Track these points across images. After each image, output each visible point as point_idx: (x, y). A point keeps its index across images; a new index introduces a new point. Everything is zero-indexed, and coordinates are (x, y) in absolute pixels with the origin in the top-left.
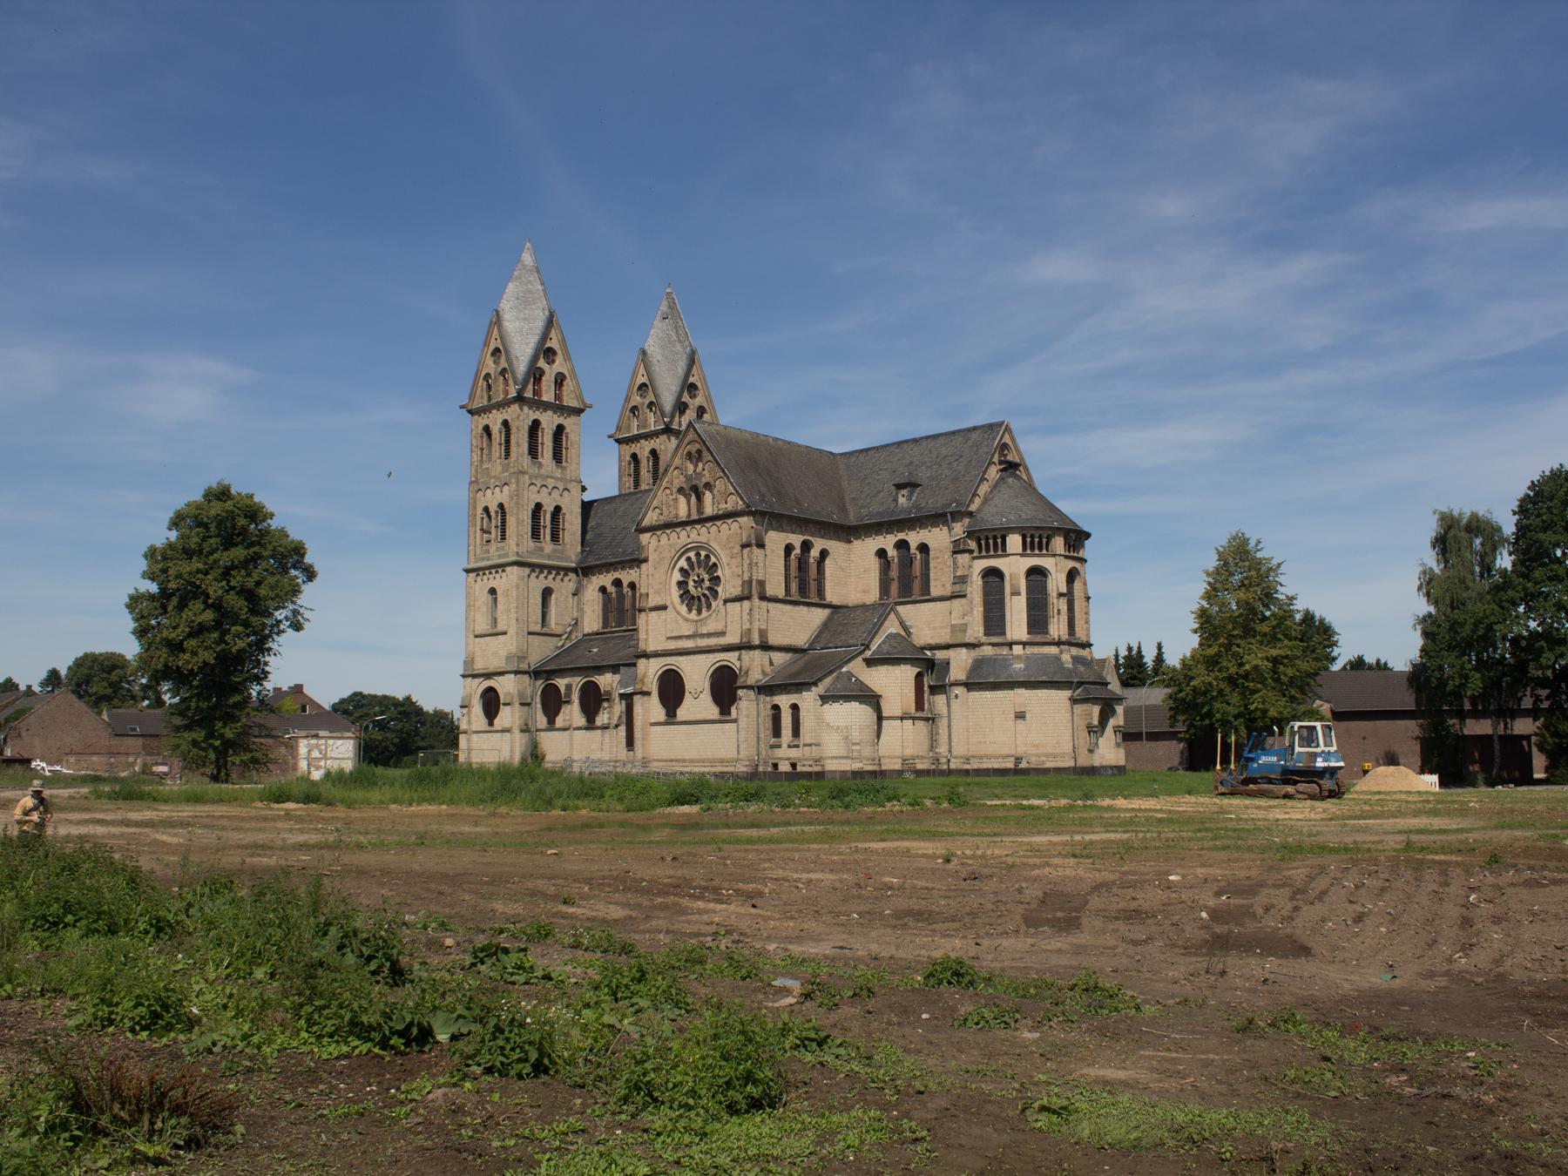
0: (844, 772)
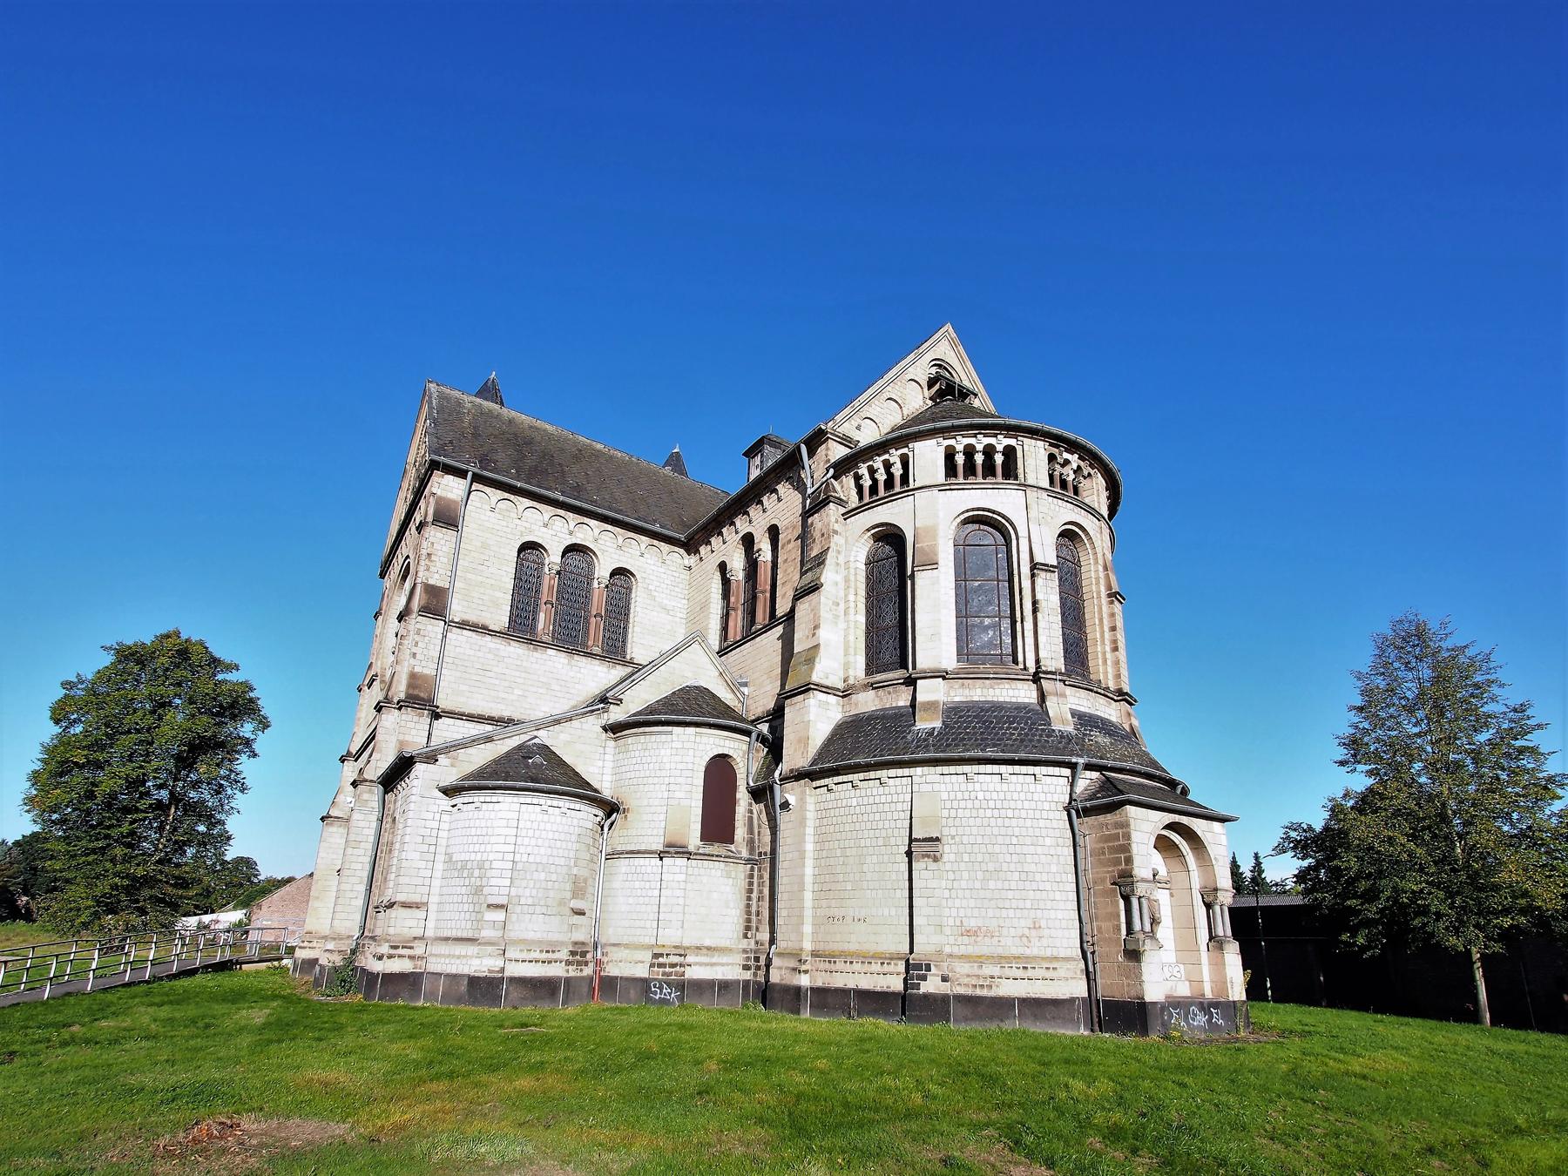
0: (454, 978)
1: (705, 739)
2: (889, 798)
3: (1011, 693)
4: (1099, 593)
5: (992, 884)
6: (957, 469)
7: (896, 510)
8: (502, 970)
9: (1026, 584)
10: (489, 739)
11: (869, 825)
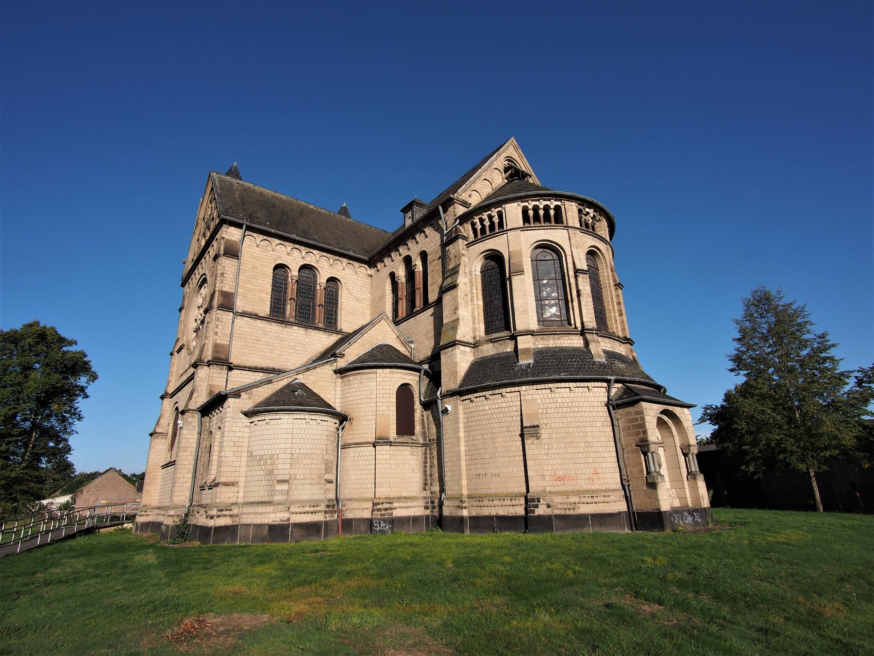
0: (259, 526)
1: (395, 375)
2: (508, 404)
3: (569, 342)
4: (610, 284)
5: (570, 450)
6: (530, 219)
7: (497, 242)
8: (289, 519)
9: (573, 281)
10: (270, 382)
11: (497, 420)
